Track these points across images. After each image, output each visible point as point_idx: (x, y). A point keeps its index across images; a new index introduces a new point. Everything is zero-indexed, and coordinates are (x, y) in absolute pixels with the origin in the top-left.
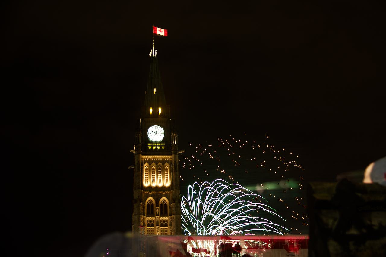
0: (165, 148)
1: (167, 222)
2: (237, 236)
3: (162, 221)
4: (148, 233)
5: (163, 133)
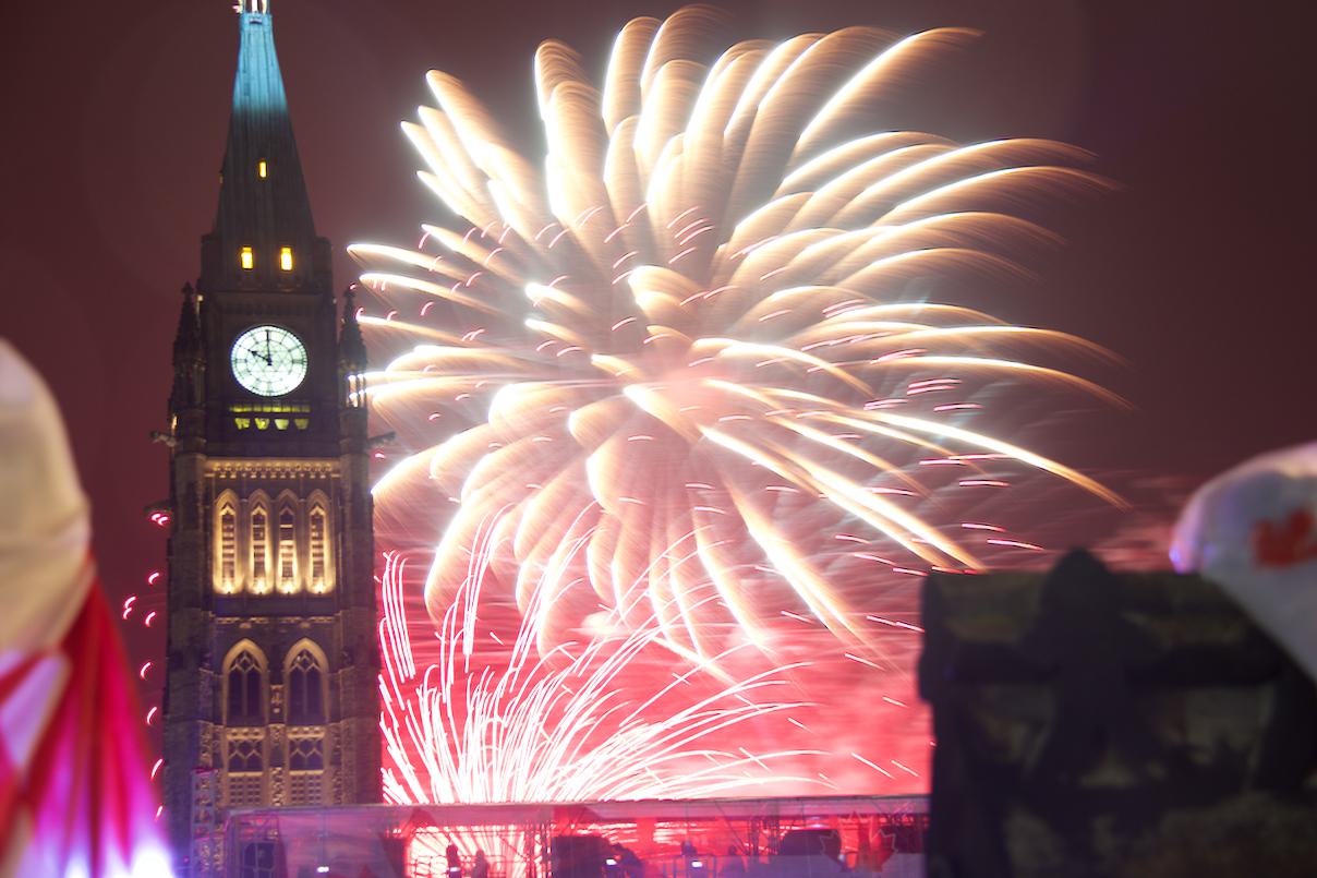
0: (309, 426)
1: (319, 748)
3: (298, 743)
4: (233, 801)
5: (302, 362)
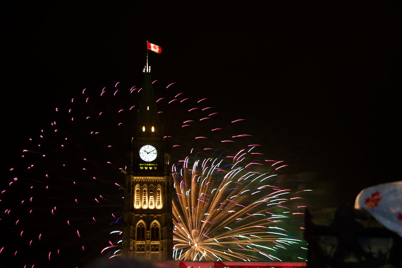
0: (157, 169)
1: (158, 247)
2: (251, 262)
3: (153, 245)
5: (156, 153)
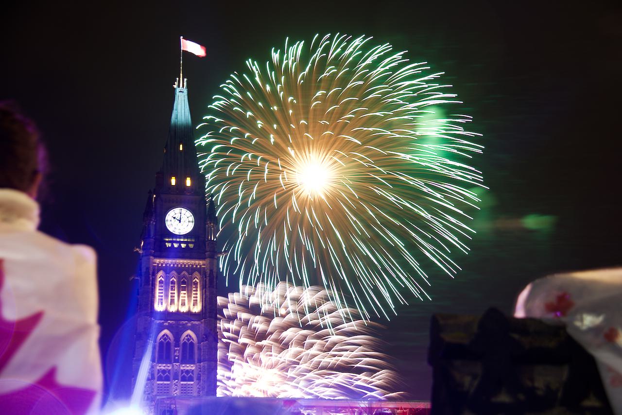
1: (193, 374)
3: (184, 371)
4: (158, 393)
